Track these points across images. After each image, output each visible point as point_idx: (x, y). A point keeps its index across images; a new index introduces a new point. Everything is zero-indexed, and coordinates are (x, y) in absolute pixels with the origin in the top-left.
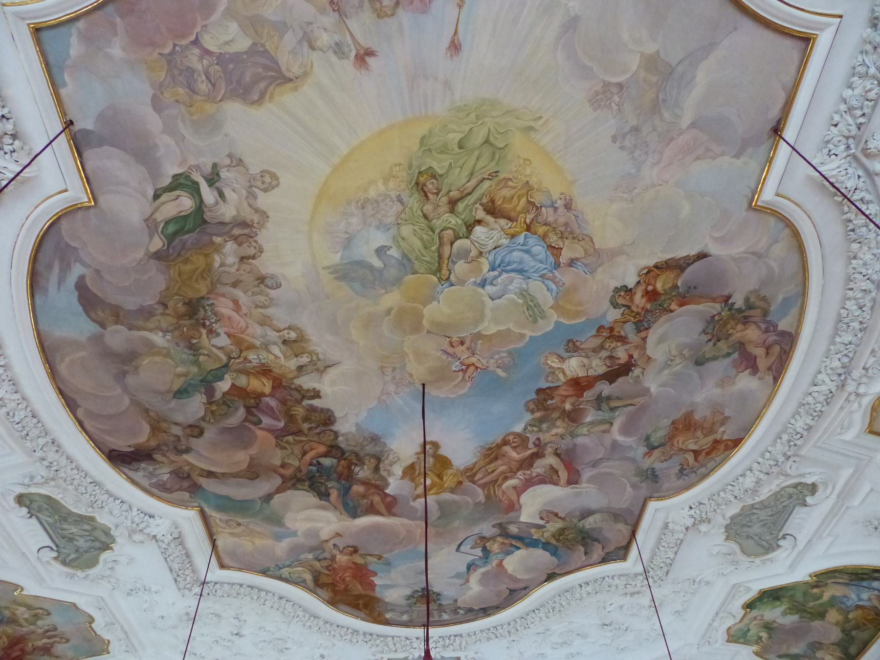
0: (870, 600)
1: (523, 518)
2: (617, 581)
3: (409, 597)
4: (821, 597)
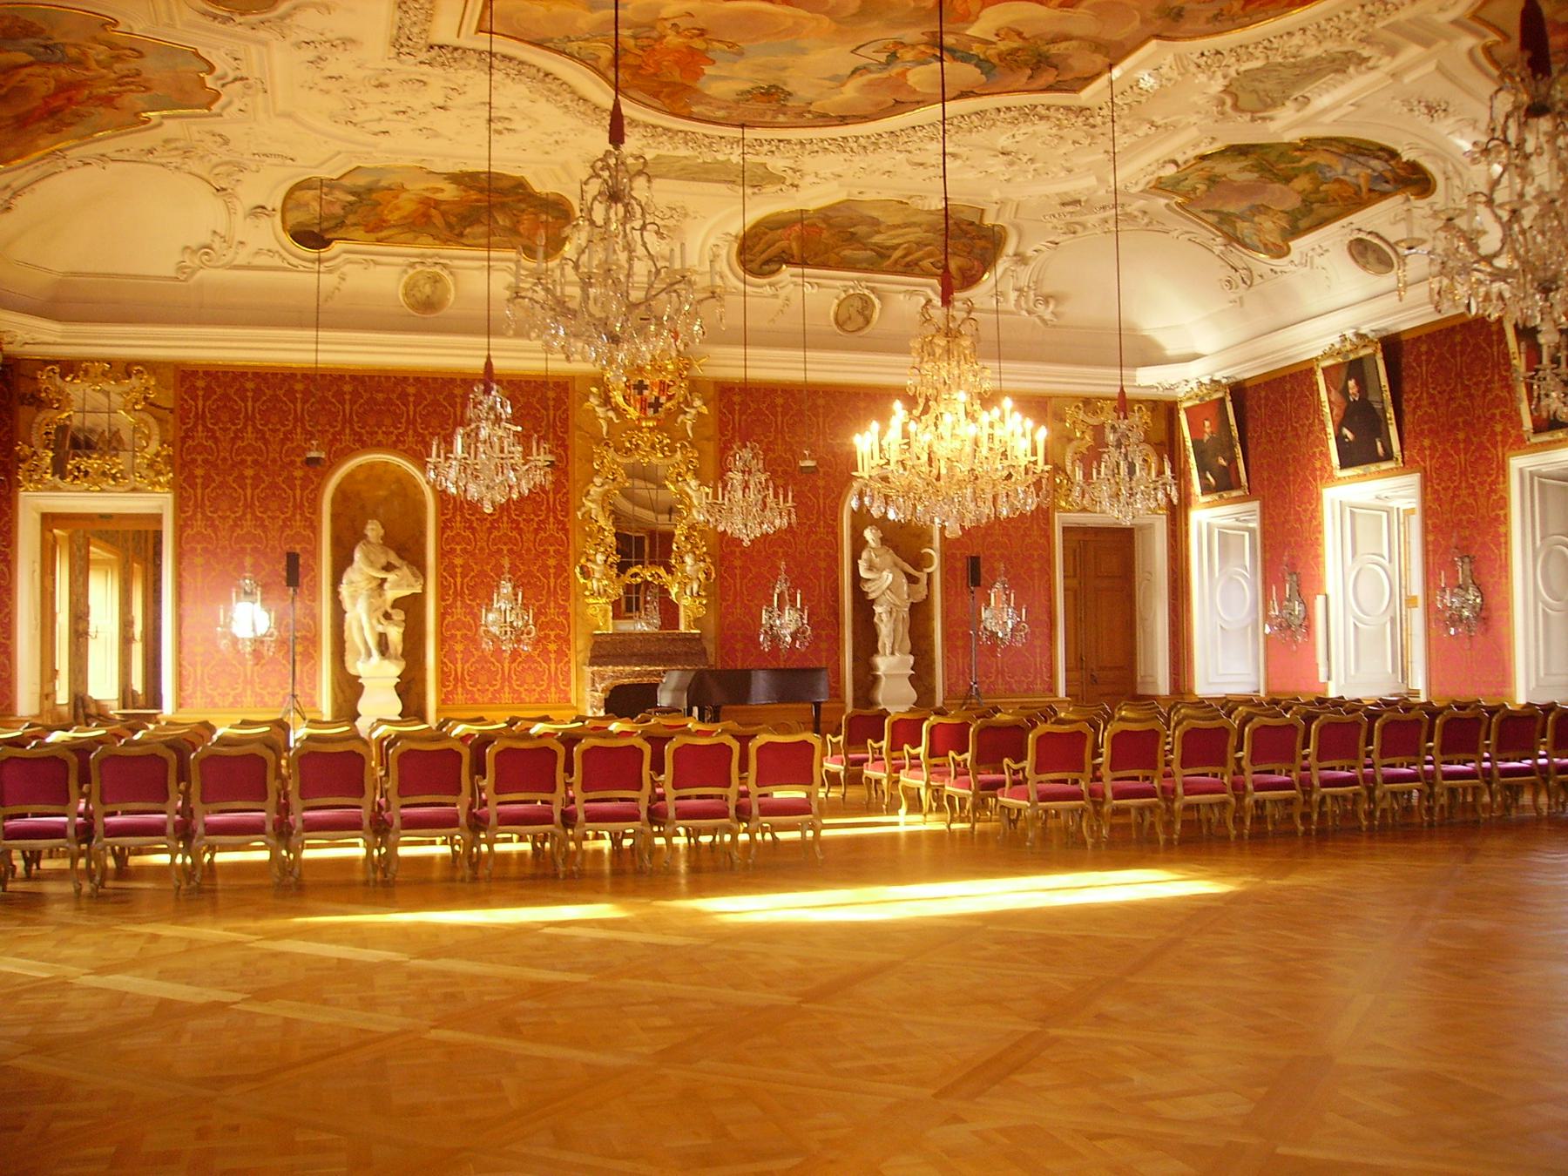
0: (1357, 176)
1: (973, 31)
2: (1052, 112)
3: (743, 93)
4: (1300, 161)
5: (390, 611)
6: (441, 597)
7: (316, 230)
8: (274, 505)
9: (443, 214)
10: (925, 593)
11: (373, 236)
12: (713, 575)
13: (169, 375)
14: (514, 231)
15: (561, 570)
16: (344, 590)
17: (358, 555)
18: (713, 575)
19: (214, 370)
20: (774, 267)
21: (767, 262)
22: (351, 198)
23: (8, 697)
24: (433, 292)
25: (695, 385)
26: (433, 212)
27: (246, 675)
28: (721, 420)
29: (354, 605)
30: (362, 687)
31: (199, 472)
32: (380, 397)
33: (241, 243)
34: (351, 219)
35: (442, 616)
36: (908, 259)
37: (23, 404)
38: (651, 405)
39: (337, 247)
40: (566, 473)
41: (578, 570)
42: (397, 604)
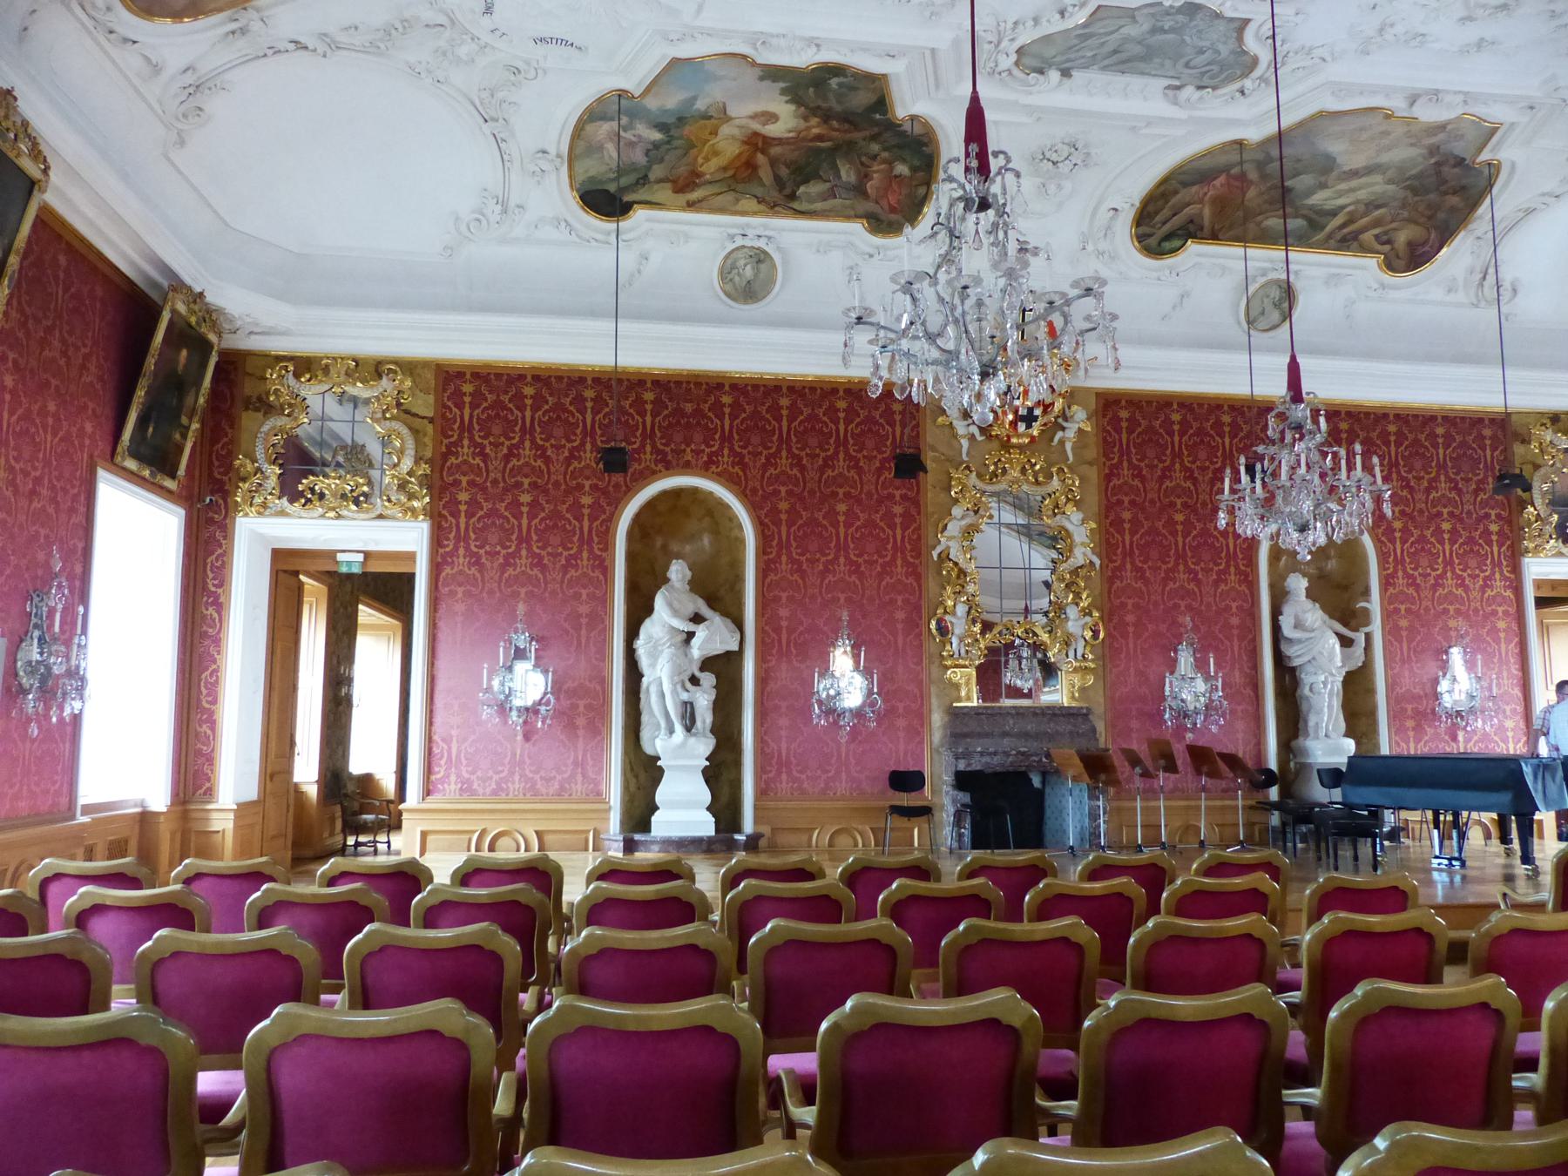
5: (698, 674)
7: (612, 188)
8: (555, 539)
9: (773, 163)
11: (683, 198)
12: (1102, 635)
13: (429, 376)
14: (859, 190)
15: (914, 624)
16: (640, 645)
17: (659, 602)
19: (485, 371)
20: (1177, 243)
22: (657, 136)
23: (209, 780)
24: (756, 275)
26: (760, 158)
27: (514, 755)
28: (1105, 439)
29: (653, 666)
30: (661, 771)
31: (463, 496)
32: (689, 407)
33: (519, 206)
34: (657, 172)
35: (762, 680)
36: (1345, 231)
37: (247, 409)
38: (1023, 418)
39: (640, 217)
40: (917, 504)
42: (708, 664)
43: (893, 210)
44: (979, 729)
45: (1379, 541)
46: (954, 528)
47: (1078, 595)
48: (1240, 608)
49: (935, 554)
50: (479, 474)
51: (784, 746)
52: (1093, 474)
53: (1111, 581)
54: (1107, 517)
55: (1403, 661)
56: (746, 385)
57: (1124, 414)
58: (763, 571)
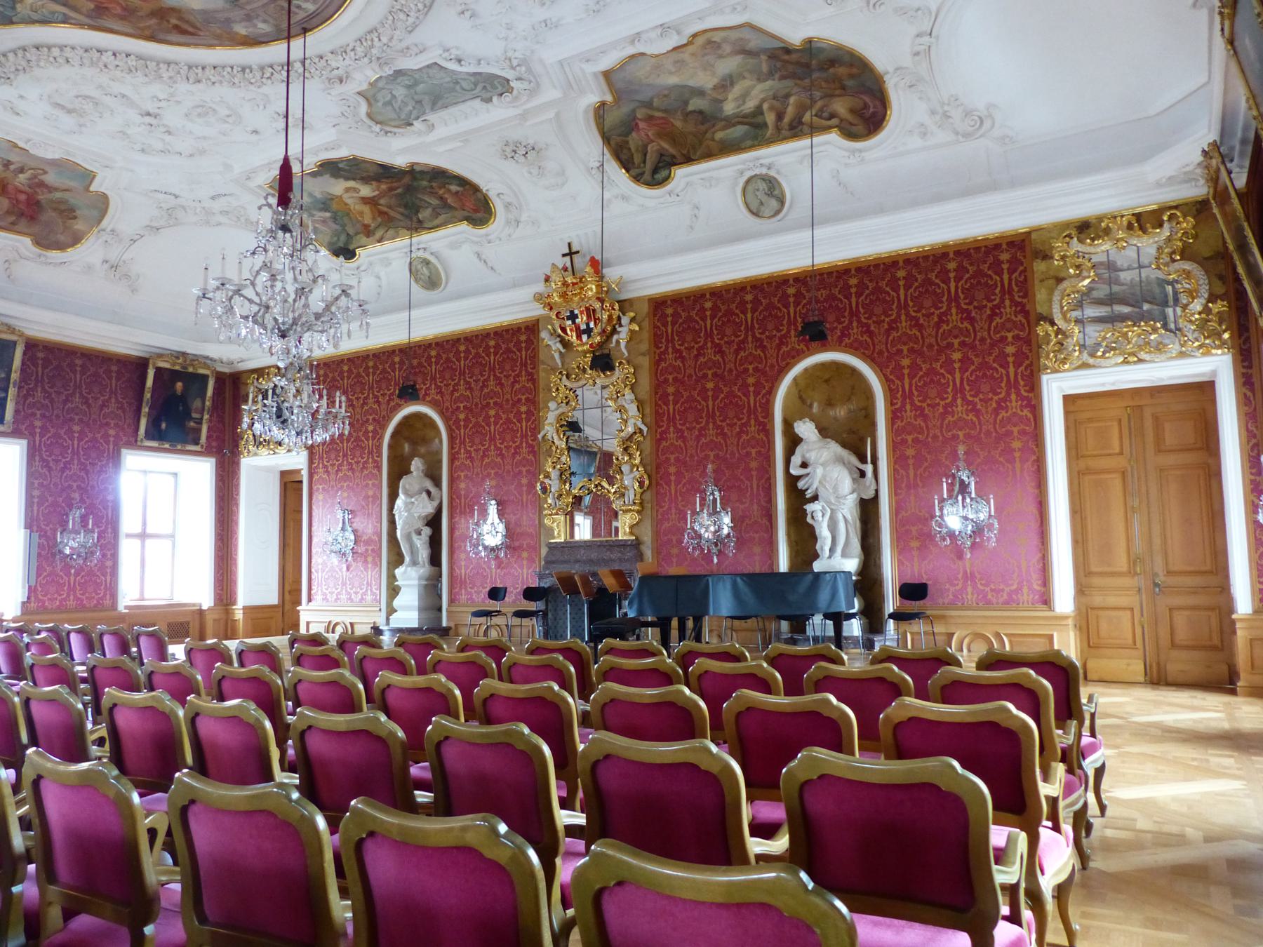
6: (451, 517)
10: (873, 487)
12: (647, 482)
14: (445, 205)
18: (647, 482)
20: (664, 173)
21: (655, 170)
25: (624, 305)
28: (655, 334)
32: (415, 362)
35: (452, 530)
36: (787, 120)
38: (584, 332)
41: (539, 487)
43: (476, 211)
44: (561, 558)
45: (887, 379)
46: (551, 417)
47: (631, 456)
48: (759, 453)
49: (540, 436)
50: (968, 335)
51: (463, 571)
52: (645, 362)
53: (659, 441)
54: (656, 393)
55: (909, 487)
56: (918, 258)
57: (669, 311)
58: (453, 458)
